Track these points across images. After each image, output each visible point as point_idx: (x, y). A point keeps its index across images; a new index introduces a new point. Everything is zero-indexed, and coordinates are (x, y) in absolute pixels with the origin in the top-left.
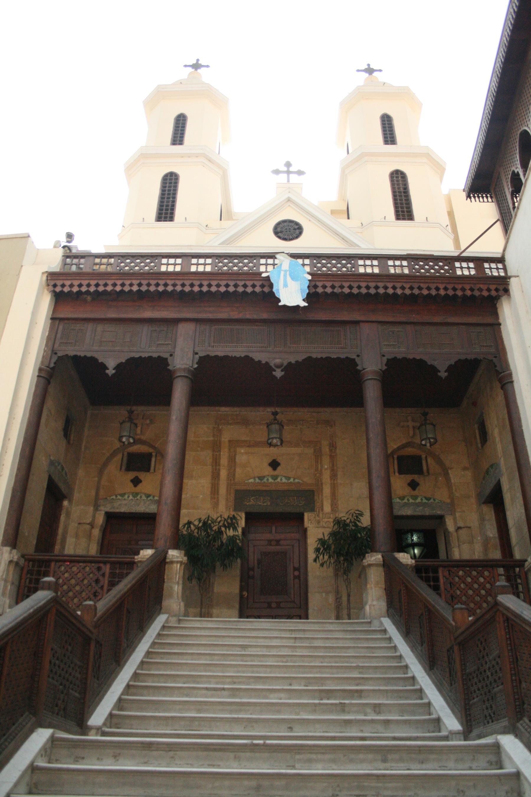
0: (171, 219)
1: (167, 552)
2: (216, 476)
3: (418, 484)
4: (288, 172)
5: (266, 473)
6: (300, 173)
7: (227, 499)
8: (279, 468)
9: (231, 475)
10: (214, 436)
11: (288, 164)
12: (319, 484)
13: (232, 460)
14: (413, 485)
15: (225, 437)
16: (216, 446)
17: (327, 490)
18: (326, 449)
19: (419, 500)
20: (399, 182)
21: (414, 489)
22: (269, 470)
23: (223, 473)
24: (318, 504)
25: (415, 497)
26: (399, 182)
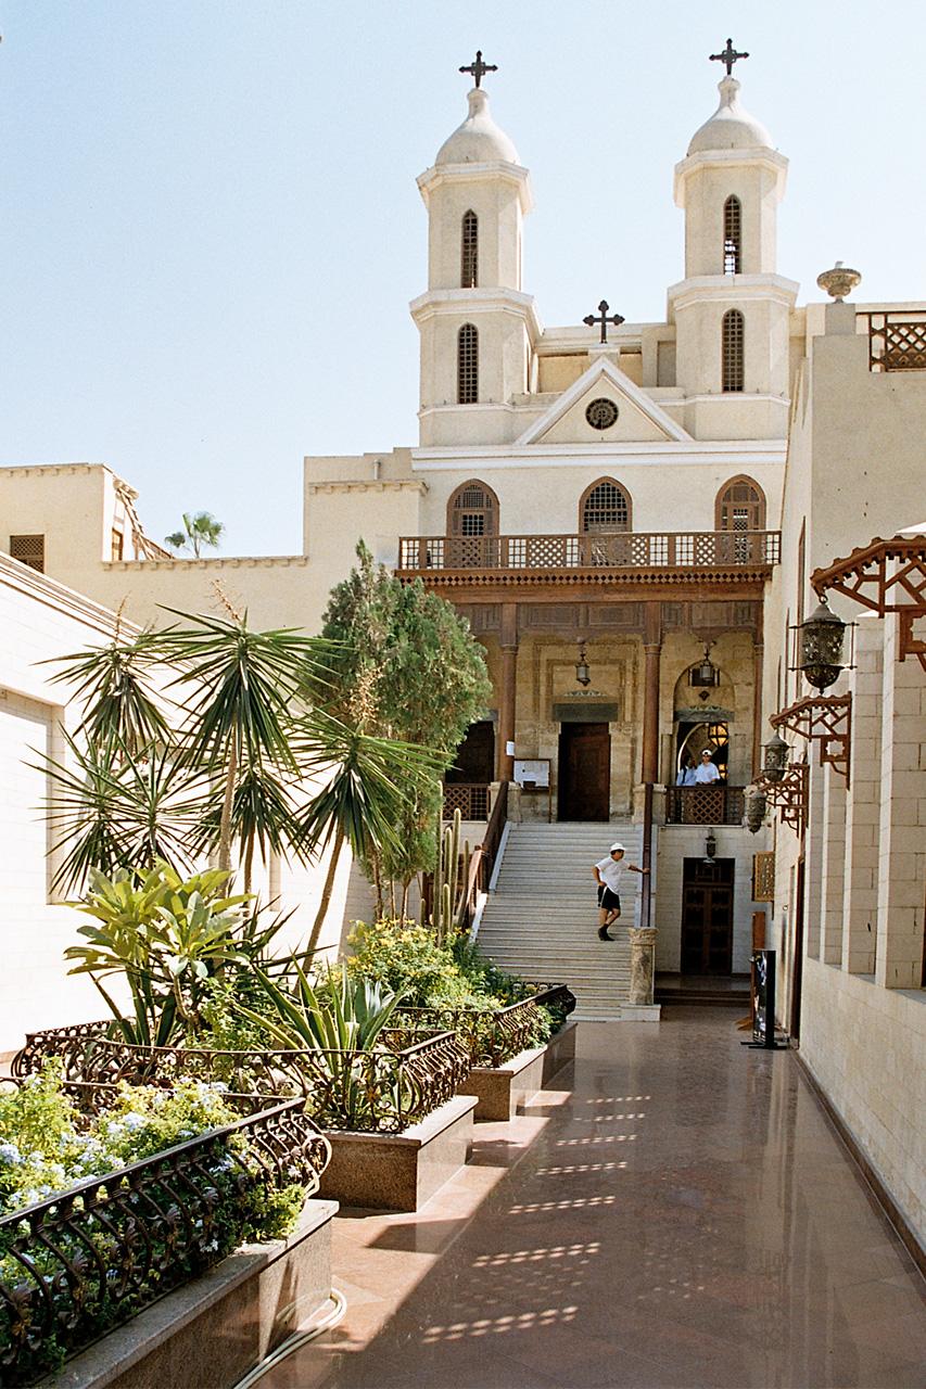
0: (475, 400)
1: (508, 784)
2: (537, 691)
3: (708, 695)
4: (604, 320)
5: (578, 689)
6: (618, 320)
7: (547, 712)
8: (589, 685)
9: (550, 690)
10: (534, 656)
11: (604, 306)
12: (622, 698)
13: (550, 677)
14: (704, 696)
15: (544, 657)
16: (536, 665)
17: (628, 703)
18: (629, 667)
19: (707, 709)
20: (733, 324)
21: (704, 699)
22: (580, 686)
23: (543, 690)
24: (620, 715)
25: (704, 707)
26: (733, 324)
